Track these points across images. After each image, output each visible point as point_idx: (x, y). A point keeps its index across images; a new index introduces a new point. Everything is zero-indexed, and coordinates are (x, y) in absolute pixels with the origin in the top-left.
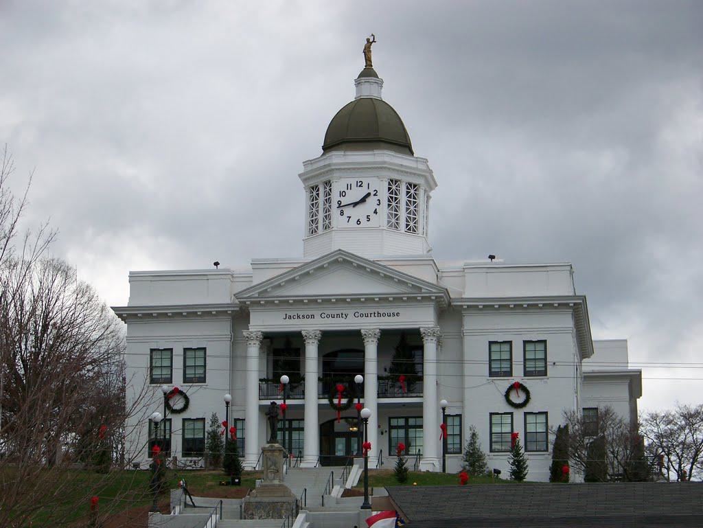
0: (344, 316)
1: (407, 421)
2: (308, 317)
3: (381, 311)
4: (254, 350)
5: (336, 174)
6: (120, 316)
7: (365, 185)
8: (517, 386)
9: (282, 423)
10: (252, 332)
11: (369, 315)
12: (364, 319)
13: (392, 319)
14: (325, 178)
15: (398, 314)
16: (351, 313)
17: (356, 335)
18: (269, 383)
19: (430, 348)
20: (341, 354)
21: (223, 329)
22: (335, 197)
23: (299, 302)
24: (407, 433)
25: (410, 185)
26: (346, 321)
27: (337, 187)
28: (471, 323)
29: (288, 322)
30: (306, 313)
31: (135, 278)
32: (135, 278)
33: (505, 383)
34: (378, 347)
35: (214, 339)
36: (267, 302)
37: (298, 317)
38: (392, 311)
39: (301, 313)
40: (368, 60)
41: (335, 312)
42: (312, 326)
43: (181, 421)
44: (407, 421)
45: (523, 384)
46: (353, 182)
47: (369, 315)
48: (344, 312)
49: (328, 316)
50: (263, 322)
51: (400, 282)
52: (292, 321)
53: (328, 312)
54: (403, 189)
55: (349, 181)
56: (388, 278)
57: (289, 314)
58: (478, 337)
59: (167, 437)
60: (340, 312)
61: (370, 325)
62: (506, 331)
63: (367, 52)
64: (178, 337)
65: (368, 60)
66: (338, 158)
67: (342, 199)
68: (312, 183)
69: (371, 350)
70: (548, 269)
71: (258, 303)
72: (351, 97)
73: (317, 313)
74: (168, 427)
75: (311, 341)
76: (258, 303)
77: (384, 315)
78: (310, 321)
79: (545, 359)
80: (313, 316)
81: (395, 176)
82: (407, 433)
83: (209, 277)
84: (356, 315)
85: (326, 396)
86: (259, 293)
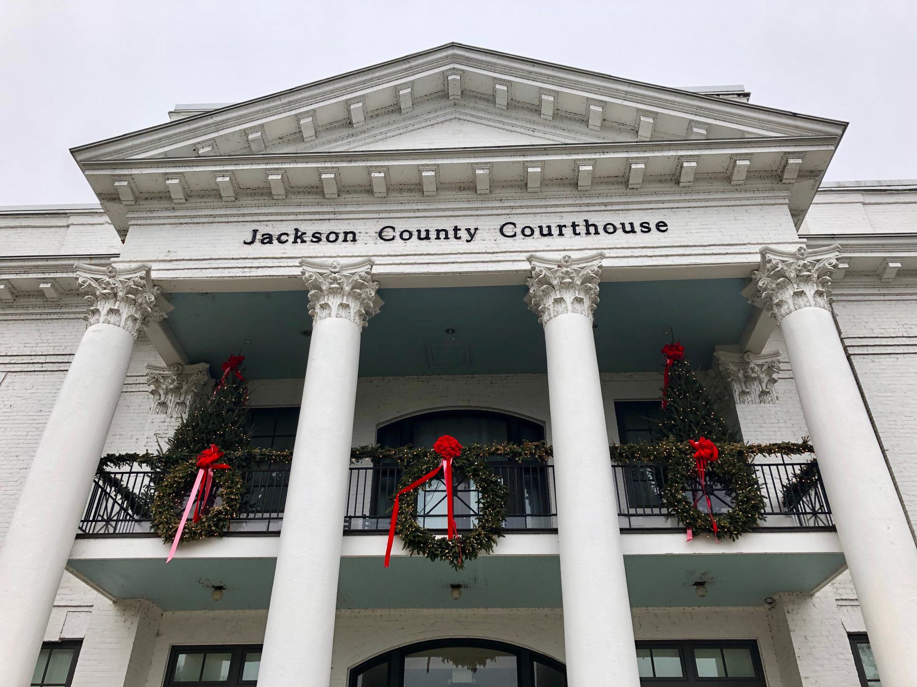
0: (463, 234)
2: (333, 238)
3: (600, 220)
11: (555, 231)
12: (537, 243)
16: (488, 227)
26: (473, 246)
29: (258, 249)
30: (324, 228)
37: (299, 237)
38: (637, 219)
39: (309, 229)
42: (349, 259)
47: (555, 231)
48: (463, 224)
49: (406, 235)
52: (275, 249)
57: (263, 229)
60: (449, 225)
73: (367, 229)
75: (334, 302)
77: (610, 229)
78: (341, 248)
80: (351, 237)
83: (73, 220)
84: (508, 230)
85: (384, 524)
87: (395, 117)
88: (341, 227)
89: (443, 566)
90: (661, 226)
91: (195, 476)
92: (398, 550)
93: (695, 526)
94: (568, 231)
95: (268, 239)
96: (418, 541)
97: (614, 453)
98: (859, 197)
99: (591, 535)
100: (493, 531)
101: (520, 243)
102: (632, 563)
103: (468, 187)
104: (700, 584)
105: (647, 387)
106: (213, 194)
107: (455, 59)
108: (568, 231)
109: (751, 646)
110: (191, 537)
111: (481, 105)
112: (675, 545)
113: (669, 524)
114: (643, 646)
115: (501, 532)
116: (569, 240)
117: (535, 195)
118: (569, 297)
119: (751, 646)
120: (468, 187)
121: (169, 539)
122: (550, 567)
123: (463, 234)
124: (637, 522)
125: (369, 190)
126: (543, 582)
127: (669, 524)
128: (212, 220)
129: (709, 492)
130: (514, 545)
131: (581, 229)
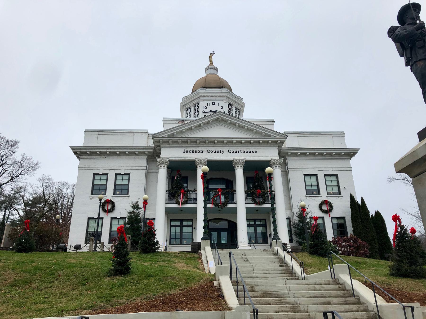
1: (255, 223)
2: (199, 152)
3: (245, 150)
4: (163, 172)
5: (202, 99)
6: (75, 153)
7: (216, 104)
8: (325, 202)
9: (180, 220)
10: (163, 159)
12: (234, 154)
13: (252, 154)
14: (195, 102)
15: (256, 152)
16: (226, 150)
17: (229, 166)
18: (173, 194)
19: (277, 173)
20: (220, 177)
21: (143, 162)
22: (201, 109)
23: (195, 142)
24: (255, 229)
25: (236, 109)
26: (224, 155)
27: (201, 106)
28: (291, 163)
30: (197, 150)
31: (87, 132)
32: (87, 132)
33: (318, 200)
34: (244, 170)
35: (136, 169)
36: (173, 142)
37: (193, 152)
39: (194, 150)
40: (211, 62)
41: (217, 150)
42: (202, 156)
43: (110, 219)
44: (255, 223)
45: (328, 200)
46: (210, 102)
48: (222, 149)
49: (212, 152)
50: (170, 154)
51: (257, 132)
52: (189, 154)
53: (211, 149)
54: (234, 109)
55: (208, 102)
56: (249, 130)
57: (186, 150)
58: (298, 169)
59: (99, 230)
60: (219, 150)
61: (239, 156)
62: (313, 168)
63: (210, 58)
64: (111, 166)
65: (211, 62)
66: (202, 91)
67: (205, 110)
68: (187, 106)
69: (239, 173)
70: (333, 135)
71: (168, 142)
72: (204, 75)
73: (205, 150)
74: (100, 223)
76: (168, 142)
79: (338, 186)
80: (202, 152)
81: (232, 102)
82: (255, 229)
83: (134, 134)
86: (169, 136)
87: (208, 125)
88: (200, 150)
89: (220, 209)
90: (256, 152)
91: (181, 194)
92: (213, 206)
93: (256, 203)
94: (240, 152)
95: (187, 152)
96: (216, 205)
97: (245, 192)
98: (297, 135)
99: (241, 203)
100: (227, 202)
101: (232, 154)
102: (247, 208)
103: (222, 142)
104: (257, 211)
105: (252, 174)
106: (177, 142)
107: (220, 114)
108: (240, 152)
109: (265, 220)
110: (182, 204)
111: (225, 122)
112: (253, 206)
113: (253, 202)
114: (248, 220)
115: (228, 204)
116: (240, 154)
117: (234, 144)
118: (240, 166)
119: (265, 220)
120: (222, 142)
121: (179, 204)
122: (235, 209)
123: (222, 152)
124: (248, 202)
125: (205, 142)
126: (234, 211)
127: (253, 202)
128: (177, 147)
129: (259, 197)
130: (230, 205)
131: (242, 152)
